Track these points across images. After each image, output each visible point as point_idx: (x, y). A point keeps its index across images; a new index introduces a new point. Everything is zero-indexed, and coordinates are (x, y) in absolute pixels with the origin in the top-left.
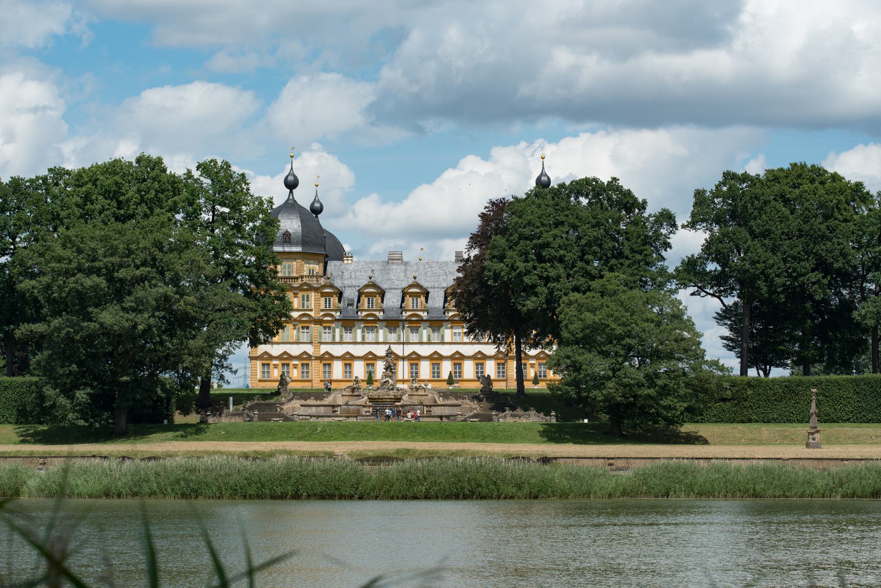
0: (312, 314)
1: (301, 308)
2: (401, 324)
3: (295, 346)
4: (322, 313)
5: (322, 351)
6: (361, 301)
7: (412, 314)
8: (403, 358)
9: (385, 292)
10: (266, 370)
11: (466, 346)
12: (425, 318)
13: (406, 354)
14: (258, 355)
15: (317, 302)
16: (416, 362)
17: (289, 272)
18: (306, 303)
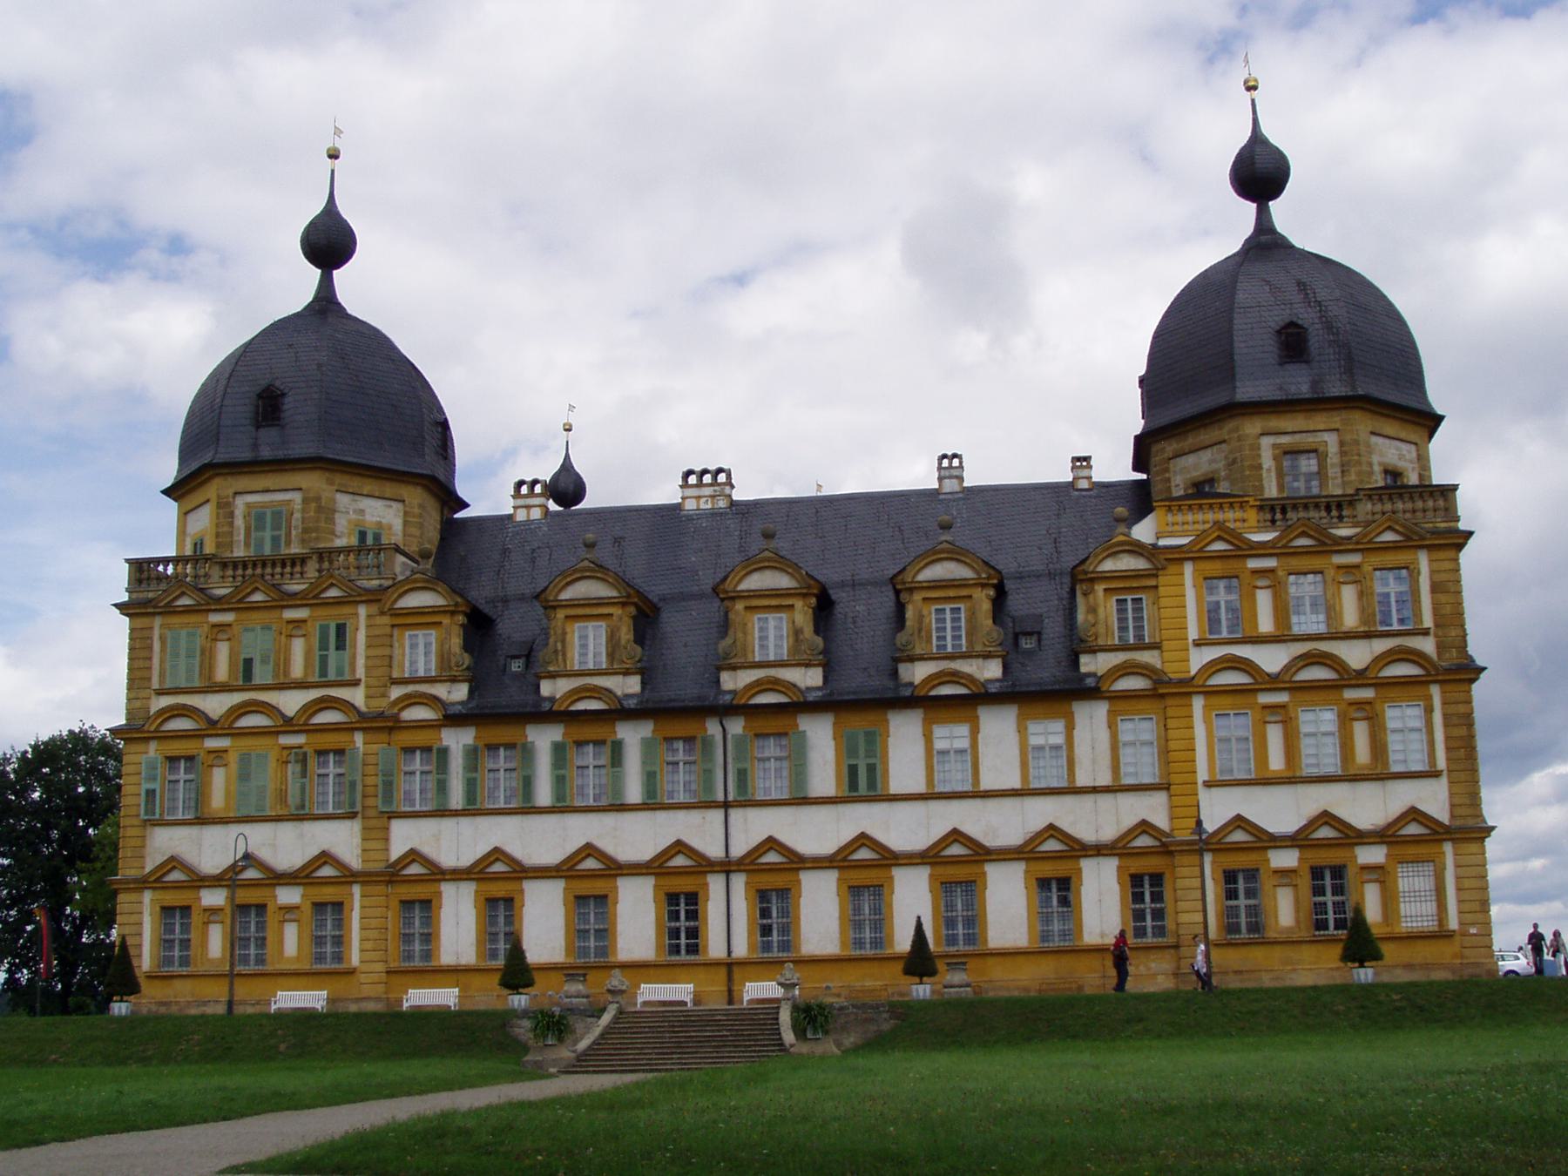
0: (357, 696)
1: (316, 679)
2: (713, 728)
3: (287, 831)
4: (396, 692)
5: (397, 851)
6: (551, 640)
7: (758, 683)
8: (727, 867)
9: (656, 609)
10: (178, 934)
11: (992, 804)
12: (811, 697)
13: (738, 850)
14: (148, 870)
15: (379, 652)
16: (778, 881)
17: (275, 540)
18: (332, 653)
